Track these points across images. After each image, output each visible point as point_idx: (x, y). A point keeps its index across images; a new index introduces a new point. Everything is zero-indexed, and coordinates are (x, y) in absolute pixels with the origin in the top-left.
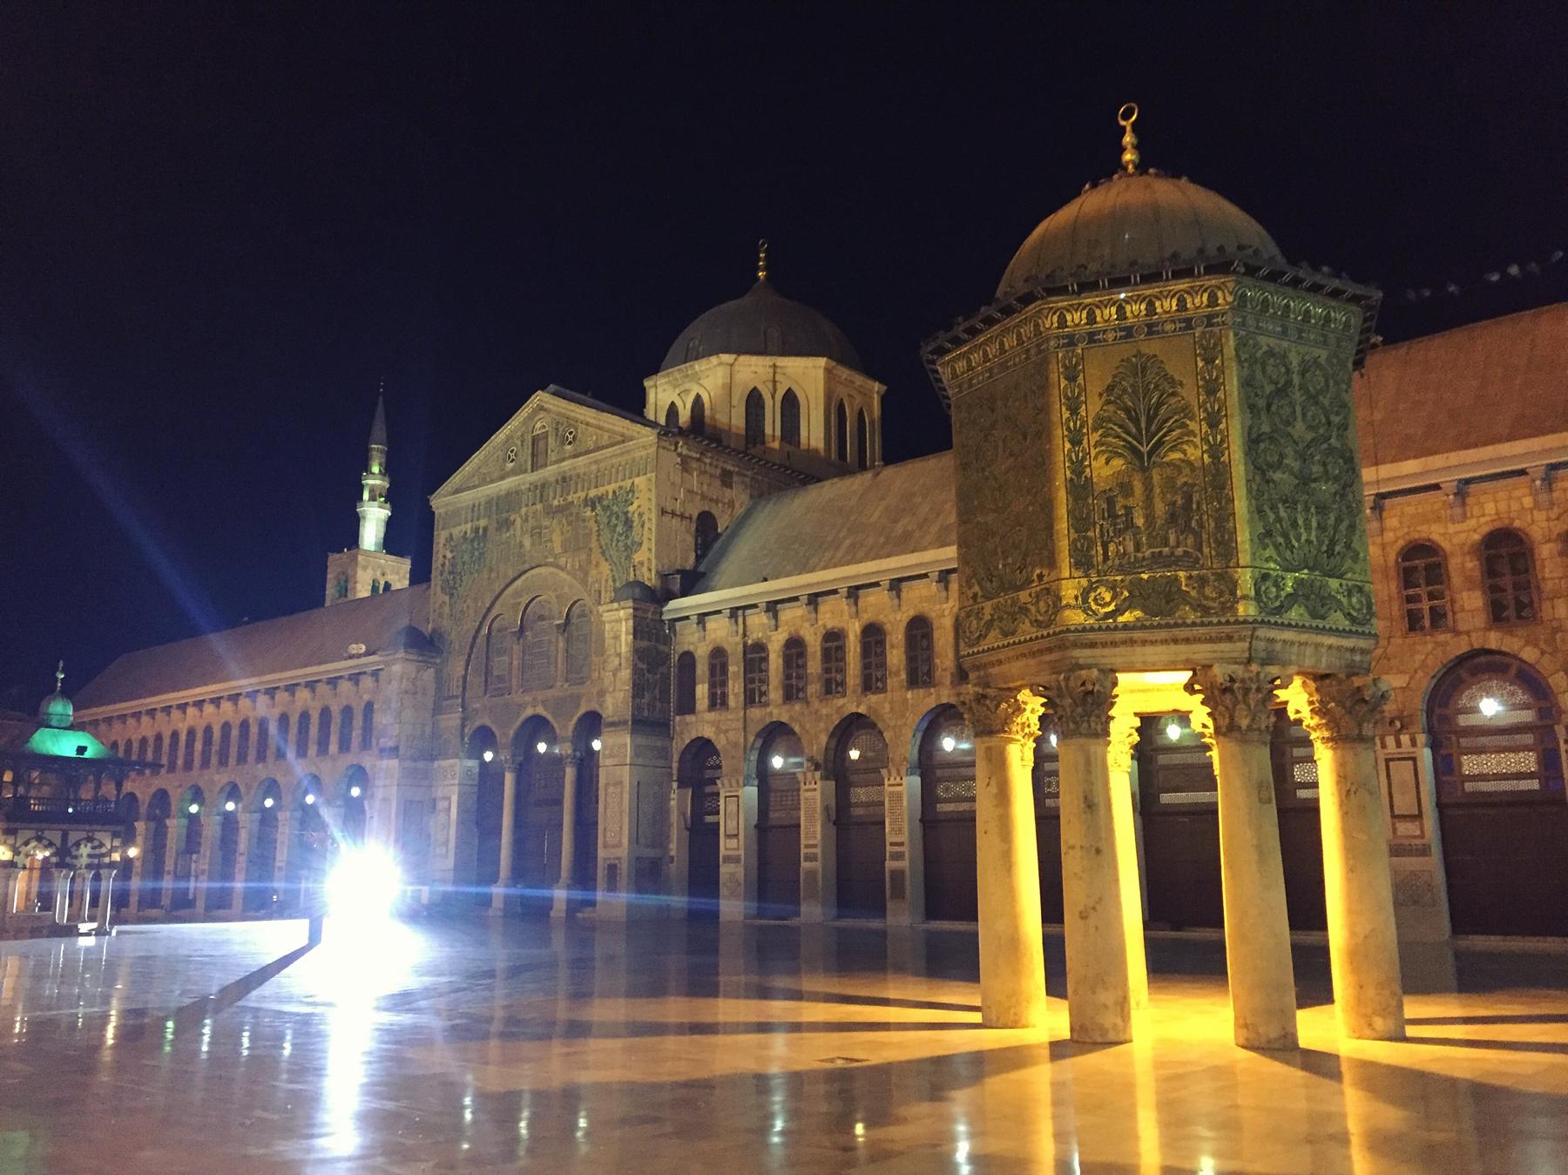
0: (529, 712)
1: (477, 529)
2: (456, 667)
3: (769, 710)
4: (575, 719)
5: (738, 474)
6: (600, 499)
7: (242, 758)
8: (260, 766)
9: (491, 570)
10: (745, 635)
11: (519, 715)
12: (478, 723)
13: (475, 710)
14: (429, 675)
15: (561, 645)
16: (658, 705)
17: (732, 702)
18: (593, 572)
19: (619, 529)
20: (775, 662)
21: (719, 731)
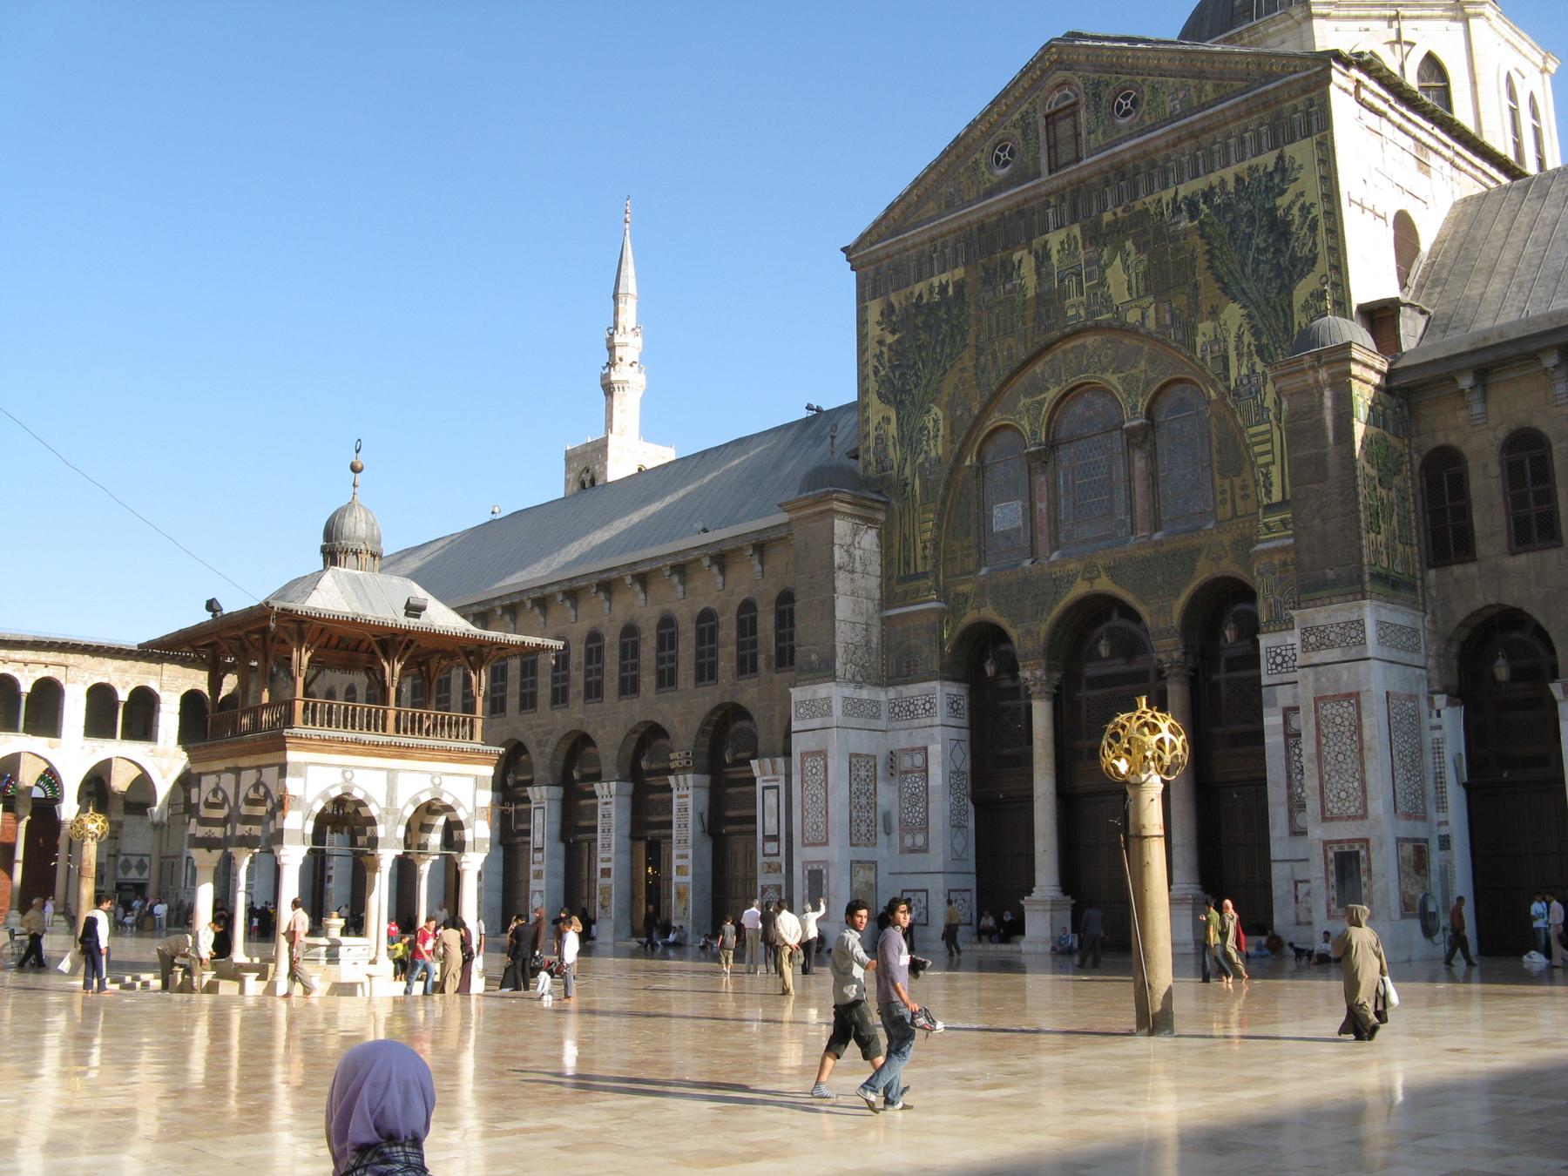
0: (1080, 589)
1: (943, 289)
4: (1183, 598)
5: (1436, 152)
6: (1208, 195)
7: (528, 702)
8: (559, 714)
9: (979, 351)
12: (970, 617)
13: (966, 597)
14: (869, 539)
15: (1140, 464)
16: (1400, 547)
18: (1205, 327)
19: (1258, 241)
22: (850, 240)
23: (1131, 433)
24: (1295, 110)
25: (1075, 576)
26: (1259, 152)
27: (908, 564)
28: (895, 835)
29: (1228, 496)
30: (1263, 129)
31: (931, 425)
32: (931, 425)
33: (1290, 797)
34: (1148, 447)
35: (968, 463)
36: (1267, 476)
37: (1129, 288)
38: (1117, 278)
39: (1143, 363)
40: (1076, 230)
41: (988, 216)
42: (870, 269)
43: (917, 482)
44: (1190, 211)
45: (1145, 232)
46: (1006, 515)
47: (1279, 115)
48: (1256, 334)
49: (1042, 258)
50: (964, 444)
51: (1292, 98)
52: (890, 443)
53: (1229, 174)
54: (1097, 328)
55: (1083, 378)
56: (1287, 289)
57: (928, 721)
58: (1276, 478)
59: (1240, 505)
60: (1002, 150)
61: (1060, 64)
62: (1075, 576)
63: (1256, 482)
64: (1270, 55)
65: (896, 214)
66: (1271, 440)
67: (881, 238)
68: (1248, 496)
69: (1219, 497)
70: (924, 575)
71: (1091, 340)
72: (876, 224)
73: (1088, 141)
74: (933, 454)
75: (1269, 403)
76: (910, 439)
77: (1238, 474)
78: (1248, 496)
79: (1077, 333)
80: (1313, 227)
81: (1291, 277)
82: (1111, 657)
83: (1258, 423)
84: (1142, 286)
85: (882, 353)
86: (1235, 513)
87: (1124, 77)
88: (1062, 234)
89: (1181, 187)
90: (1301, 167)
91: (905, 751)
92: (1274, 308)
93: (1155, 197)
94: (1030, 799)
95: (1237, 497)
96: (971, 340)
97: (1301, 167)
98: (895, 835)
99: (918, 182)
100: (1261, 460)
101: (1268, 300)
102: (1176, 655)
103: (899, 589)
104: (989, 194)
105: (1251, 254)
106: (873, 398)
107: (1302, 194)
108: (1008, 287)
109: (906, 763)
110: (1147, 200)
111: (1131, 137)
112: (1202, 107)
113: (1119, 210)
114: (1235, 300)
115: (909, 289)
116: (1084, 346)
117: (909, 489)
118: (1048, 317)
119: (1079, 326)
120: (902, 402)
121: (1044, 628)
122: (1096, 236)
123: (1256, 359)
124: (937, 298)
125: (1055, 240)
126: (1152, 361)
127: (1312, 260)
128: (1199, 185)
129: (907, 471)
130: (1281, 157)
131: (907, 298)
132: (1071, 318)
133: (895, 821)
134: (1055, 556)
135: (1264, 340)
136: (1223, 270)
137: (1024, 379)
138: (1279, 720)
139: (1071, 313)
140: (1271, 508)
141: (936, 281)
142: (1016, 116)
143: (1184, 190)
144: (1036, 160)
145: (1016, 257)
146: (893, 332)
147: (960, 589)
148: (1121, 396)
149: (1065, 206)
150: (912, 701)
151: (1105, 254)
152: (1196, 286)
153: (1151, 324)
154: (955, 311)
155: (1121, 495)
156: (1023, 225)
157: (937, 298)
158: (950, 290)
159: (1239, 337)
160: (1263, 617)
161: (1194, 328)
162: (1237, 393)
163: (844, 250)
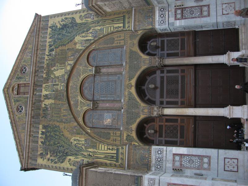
0: (133, 90)
6: (50, 46)
9: (61, 121)
11: (134, 99)
12: (134, 135)
13: (128, 135)
15: (104, 70)
18: (79, 47)
22: (19, 166)
25: (129, 92)
26: (47, 32)
27: (113, 157)
28: (203, 172)
29: (119, 42)
31: (75, 142)
32: (75, 142)
33: (199, 17)
34: (101, 68)
35: (89, 131)
36: (116, 28)
37: (62, 69)
39: (81, 68)
40: (44, 85)
41: (31, 114)
43: (90, 150)
45: (51, 64)
46: (108, 121)
47: (42, 28)
49: (46, 97)
50: (83, 130)
51: (40, 25)
52: (76, 160)
53: (48, 40)
55: (79, 87)
56: (76, 24)
57: (165, 152)
59: (122, 38)
60: (19, 109)
61: (8, 88)
62: (129, 92)
63: (118, 31)
66: (108, 27)
67: (23, 155)
68: (120, 36)
69: (118, 44)
70: (118, 150)
71: (70, 85)
73: (27, 81)
74: (83, 142)
75: (99, 28)
77: (114, 39)
78: (120, 36)
80: (66, 18)
81: (75, 23)
83: (103, 31)
84: (63, 65)
86: (123, 39)
88: (43, 90)
90: (54, 22)
91: (173, 164)
92: (79, 28)
93: (45, 61)
95: (120, 39)
96: (58, 124)
97: (54, 22)
98: (203, 172)
99: (15, 138)
100: (112, 30)
101: (77, 29)
102: (157, 59)
103: (120, 161)
105: (66, 34)
106: (62, 165)
107: (59, 21)
108: (49, 110)
109: (177, 164)
110: (45, 63)
112: (33, 48)
113: (45, 72)
114: (74, 38)
115: (39, 146)
117: (91, 154)
118: (61, 95)
119: (66, 86)
120: (66, 153)
121: (143, 105)
122: (47, 80)
123: (89, 32)
125: (44, 93)
126: (81, 64)
127: (73, 18)
128: (47, 49)
129: (86, 154)
130: (50, 27)
131: (41, 148)
132: (63, 88)
133: (198, 172)
134: (122, 101)
135: (85, 30)
136: (67, 42)
137: (73, 108)
138: (178, 21)
139: (62, 88)
140: (124, 27)
141: (40, 136)
143: (47, 53)
144: (25, 98)
145: (43, 106)
146: (47, 154)
147: (125, 138)
148: (85, 75)
149: (38, 89)
150: (157, 159)
151: (52, 76)
155: (111, 78)
156: (36, 104)
158: (44, 130)
159: (83, 37)
160: (151, 27)
161: (78, 49)
162: (95, 37)
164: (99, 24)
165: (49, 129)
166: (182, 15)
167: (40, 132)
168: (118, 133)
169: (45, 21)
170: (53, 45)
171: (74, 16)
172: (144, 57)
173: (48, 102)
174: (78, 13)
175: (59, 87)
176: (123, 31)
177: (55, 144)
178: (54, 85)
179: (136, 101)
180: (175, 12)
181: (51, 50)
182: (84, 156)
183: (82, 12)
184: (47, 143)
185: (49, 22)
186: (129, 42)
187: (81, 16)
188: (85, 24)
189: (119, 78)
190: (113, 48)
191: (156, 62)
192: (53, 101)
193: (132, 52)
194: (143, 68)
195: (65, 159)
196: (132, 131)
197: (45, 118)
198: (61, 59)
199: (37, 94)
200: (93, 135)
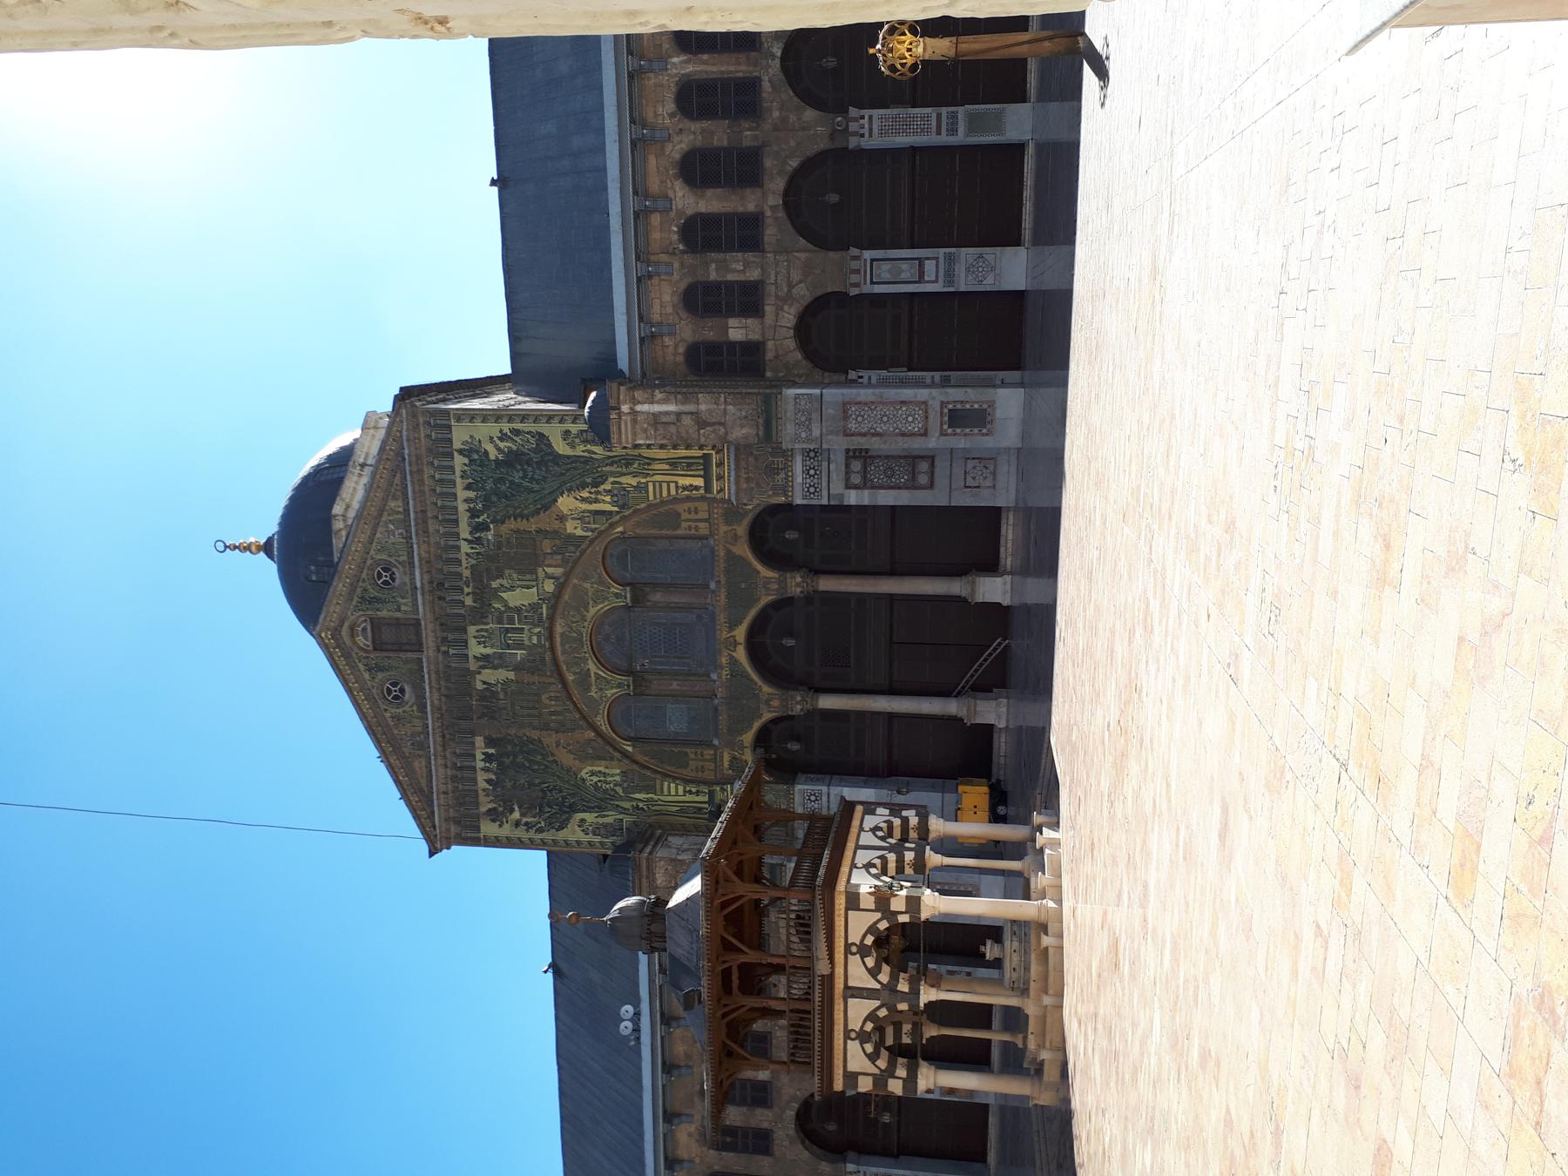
0: (741, 654)
1: (488, 758)
2: (674, 793)
3: (768, 213)
4: (759, 567)
6: (474, 514)
9: (546, 727)
10: (673, 254)
13: (734, 758)
14: (675, 841)
15: (657, 597)
17: (754, 275)
18: (573, 528)
19: (517, 477)
20: (712, 202)
21: (788, 298)
22: (424, 847)
23: (635, 599)
24: (429, 436)
26: (452, 468)
30: (436, 463)
31: (595, 779)
32: (595, 779)
34: (647, 589)
35: (630, 749)
36: (685, 488)
38: (518, 597)
39: (587, 585)
42: (454, 829)
43: (637, 796)
44: (482, 530)
48: (583, 486)
50: (615, 749)
52: (601, 820)
54: (551, 618)
56: (557, 458)
57: (825, 799)
58: (687, 481)
59: (699, 516)
62: (731, 657)
63: (688, 498)
64: (382, 449)
65: (414, 798)
70: (711, 794)
71: (559, 629)
72: (417, 817)
74: (618, 778)
76: (602, 801)
77: (679, 515)
79: (551, 638)
80: (517, 432)
82: (791, 635)
84: (528, 577)
85: (526, 824)
87: (364, 575)
88: (472, 642)
89: (462, 535)
93: (463, 558)
94: (891, 717)
96: (535, 734)
100: (673, 492)
104: (422, 708)
106: (562, 835)
111: (412, 574)
112: (407, 511)
113: (467, 590)
116: (562, 634)
120: (570, 806)
121: (766, 689)
122: (480, 614)
124: (494, 765)
126: (585, 578)
128: (464, 519)
130: (460, 452)
134: (714, 676)
137: (575, 692)
138: (853, 492)
140: (708, 487)
141: (480, 764)
142: (367, 676)
144: (406, 662)
145: (479, 686)
146: (512, 811)
147: (726, 764)
149: (450, 637)
152: (539, 531)
153: (558, 571)
154: (510, 748)
157: (494, 765)
159: (583, 500)
163: (431, 854)
164: (631, 469)
165: (510, 748)
166: (864, 478)
167: (479, 756)
168: (709, 753)
169: (436, 426)
170: (482, 512)
171: (543, 428)
172: (765, 572)
173: (490, 676)
174: (556, 419)
175: (525, 636)
176: (703, 498)
177: (531, 784)
178: (507, 630)
179: (751, 680)
180: (847, 466)
181: (479, 528)
182: (624, 811)
183: (569, 419)
184: (508, 784)
185: (455, 434)
186: (724, 528)
187: (567, 433)
188: (586, 461)
189: (699, 617)
190: (677, 537)
191: (796, 584)
192: (511, 675)
193: (733, 560)
194: (765, 600)
195: (568, 820)
196: (743, 747)
197: (492, 718)
198: (523, 558)
199: (452, 652)
200: (639, 757)
